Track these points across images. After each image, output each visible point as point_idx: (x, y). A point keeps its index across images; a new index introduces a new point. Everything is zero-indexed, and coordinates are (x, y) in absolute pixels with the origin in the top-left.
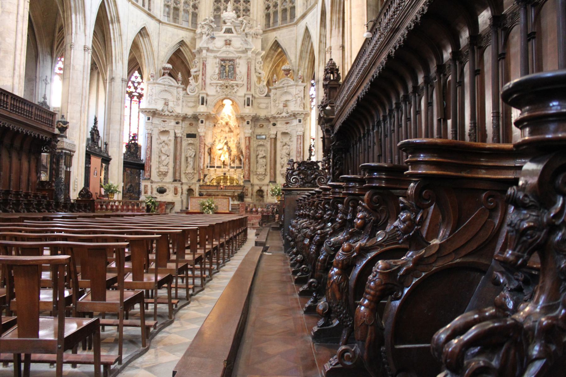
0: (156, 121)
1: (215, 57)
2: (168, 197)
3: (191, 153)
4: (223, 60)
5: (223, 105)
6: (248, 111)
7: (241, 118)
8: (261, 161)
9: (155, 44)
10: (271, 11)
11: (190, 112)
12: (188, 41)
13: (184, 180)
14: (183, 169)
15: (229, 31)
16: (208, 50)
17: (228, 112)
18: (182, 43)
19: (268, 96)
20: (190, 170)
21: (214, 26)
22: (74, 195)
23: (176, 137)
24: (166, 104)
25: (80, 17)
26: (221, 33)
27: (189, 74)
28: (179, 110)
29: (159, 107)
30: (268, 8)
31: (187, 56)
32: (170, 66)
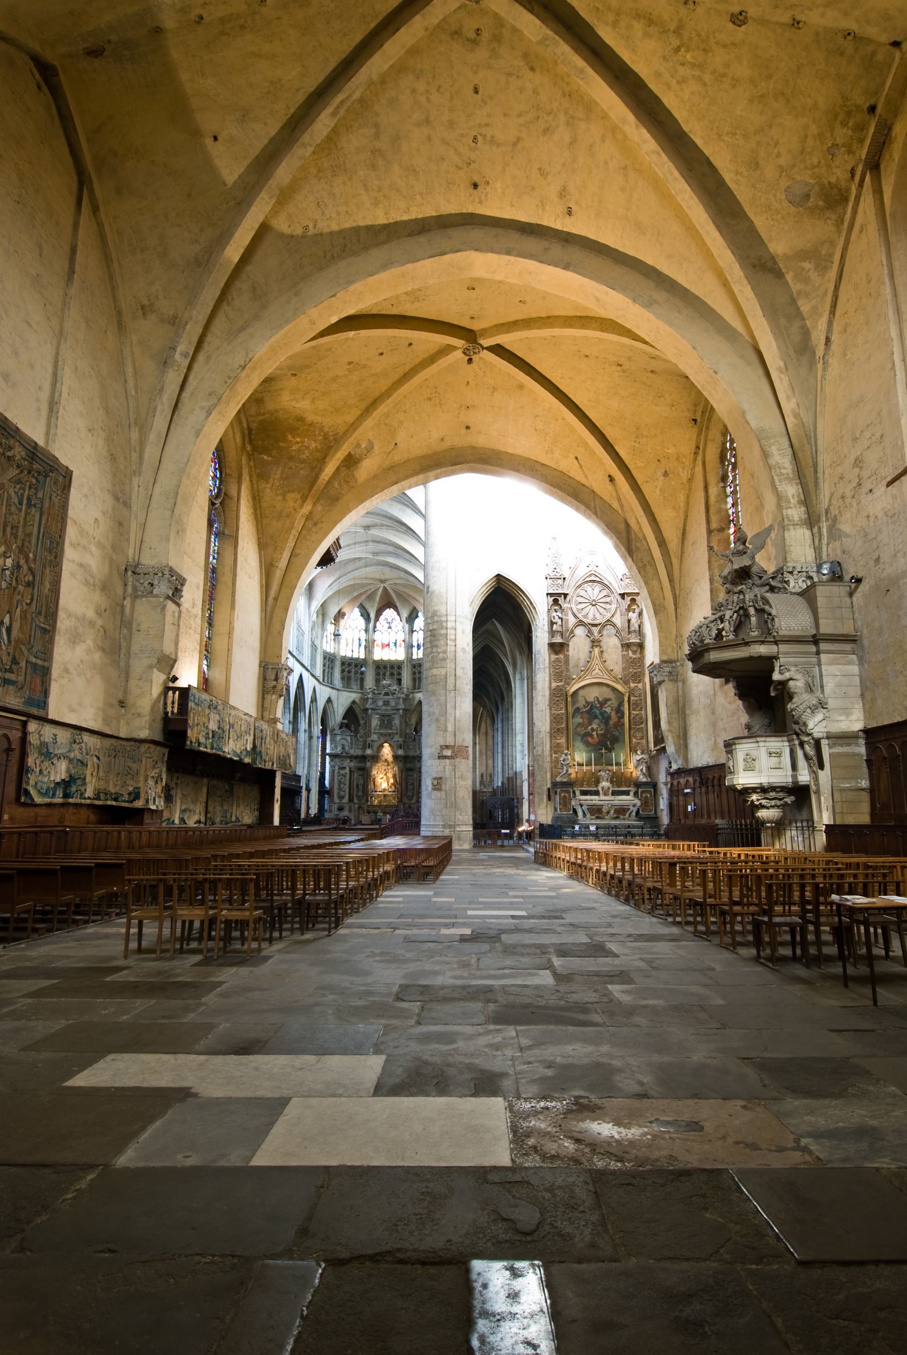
0: (337, 760)
1: (378, 714)
2: (346, 813)
3: (361, 782)
4: (383, 716)
5: (383, 746)
6: (400, 752)
7: (395, 757)
8: (410, 787)
9: (335, 706)
10: (417, 676)
11: (359, 752)
12: (357, 701)
13: (356, 801)
14: (355, 792)
15: (386, 694)
16: (372, 709)
17: (387, 751)
18: (354, 702)
19: (414, 740)
20: (360, 793)
21: (376, 692)
22: (303, 816)
23: (350, 771)
24: (343, 748)
25: (302, 714)
26: (381, 696)
27: (359, 725)
28: (352, 752)
29: (339, 750)
30: (414, 673)
31: (357, 710)
32: (346, 721)
